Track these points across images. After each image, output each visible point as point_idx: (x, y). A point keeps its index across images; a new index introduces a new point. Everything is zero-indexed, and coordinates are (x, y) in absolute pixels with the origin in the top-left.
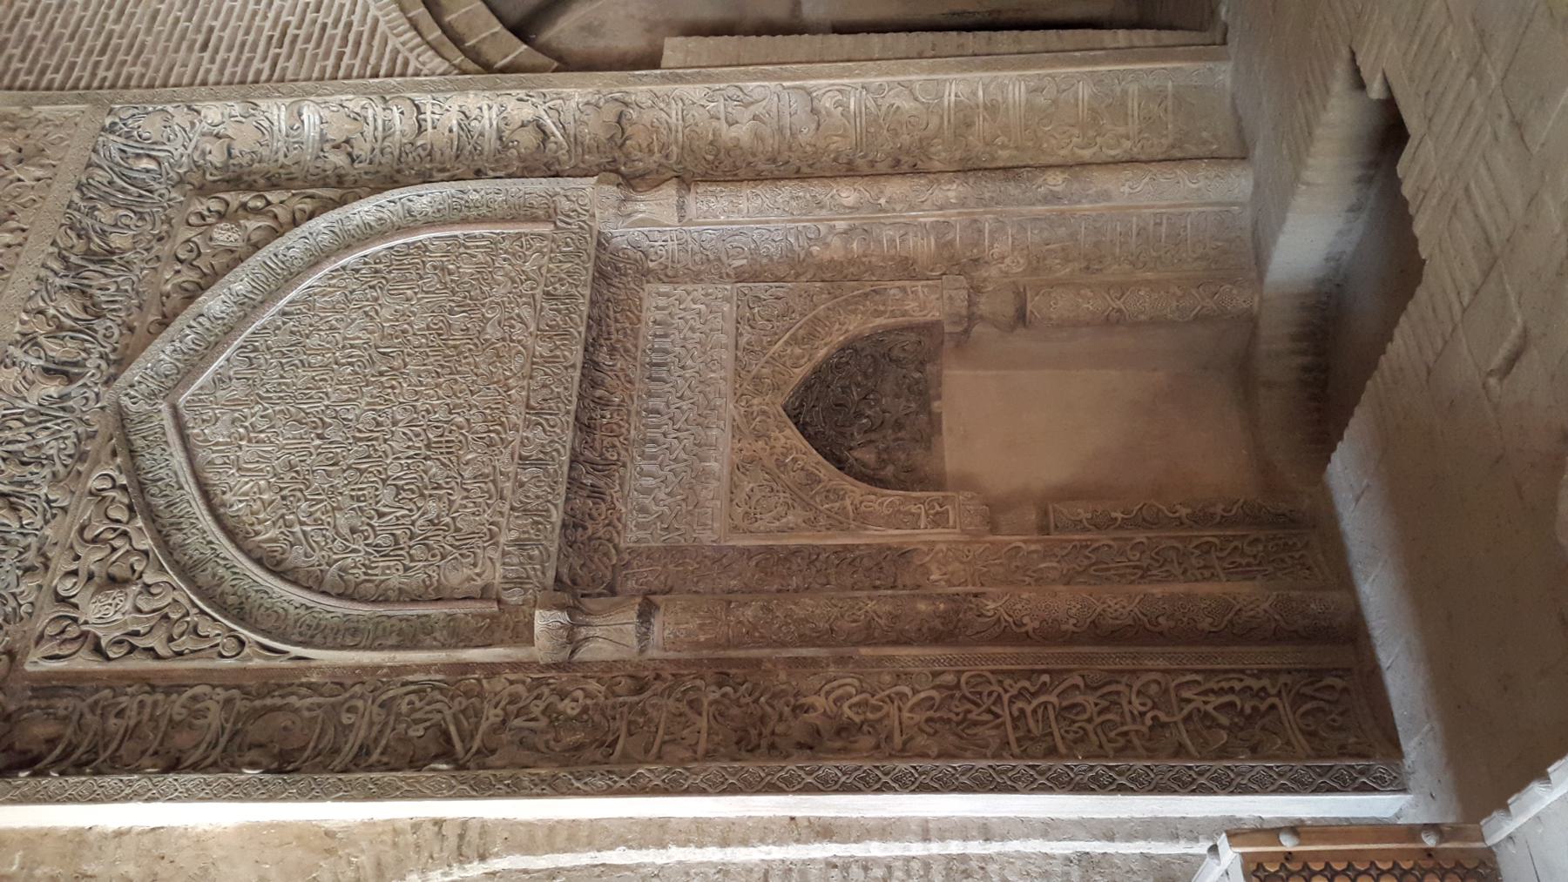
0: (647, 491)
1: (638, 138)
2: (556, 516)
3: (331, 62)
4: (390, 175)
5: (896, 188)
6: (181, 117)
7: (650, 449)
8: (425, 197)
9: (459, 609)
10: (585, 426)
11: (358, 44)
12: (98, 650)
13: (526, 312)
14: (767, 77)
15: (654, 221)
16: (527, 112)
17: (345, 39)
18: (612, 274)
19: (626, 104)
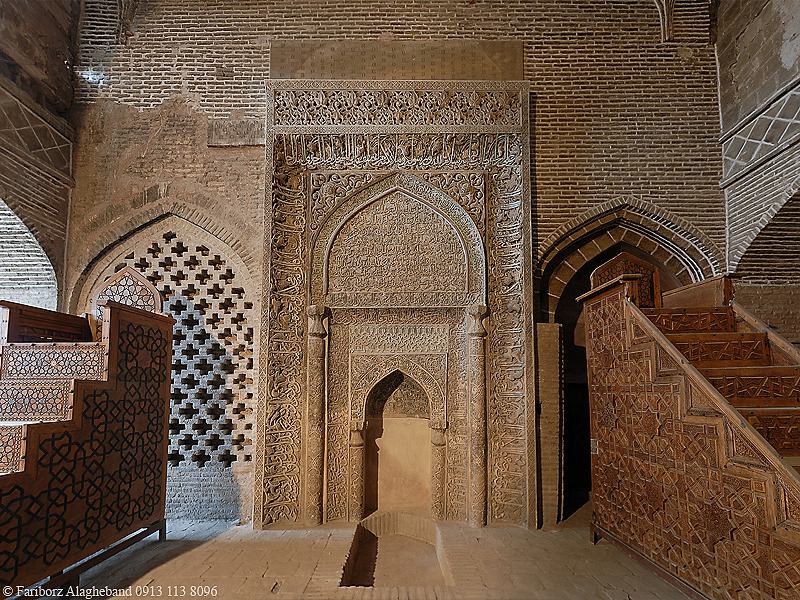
0: (368, 331)
1: (510, 318)
2: (355, 306)
3: (552, 204)
4: (488, 238)
5: (477, 406)
6: (518, 159)
7: (383, 331)
8: (479, 248)
9: (325, 284)
10: (388, 311)
11: (562, 212)
12: (315, 191)
13: (432, 288)
14: (529, 362)
15: (471, 325)
16: (517, 278)
17: (566, 206)
18: (453, 313)
19: (519, 313)
